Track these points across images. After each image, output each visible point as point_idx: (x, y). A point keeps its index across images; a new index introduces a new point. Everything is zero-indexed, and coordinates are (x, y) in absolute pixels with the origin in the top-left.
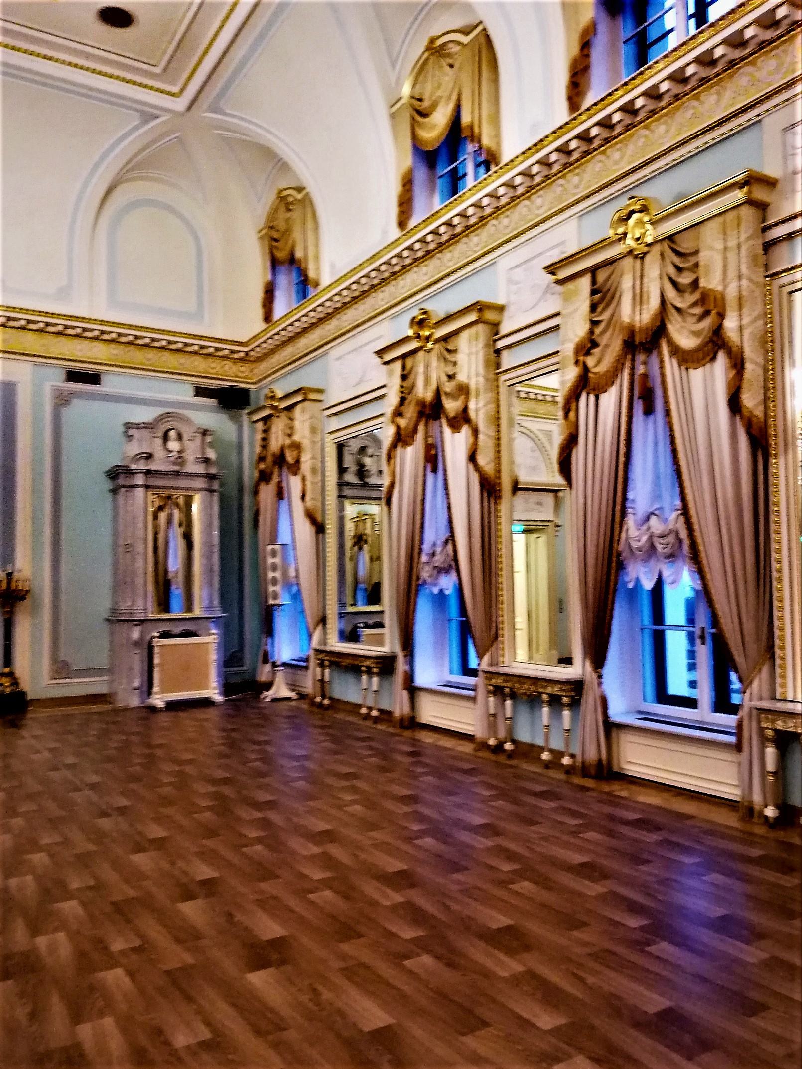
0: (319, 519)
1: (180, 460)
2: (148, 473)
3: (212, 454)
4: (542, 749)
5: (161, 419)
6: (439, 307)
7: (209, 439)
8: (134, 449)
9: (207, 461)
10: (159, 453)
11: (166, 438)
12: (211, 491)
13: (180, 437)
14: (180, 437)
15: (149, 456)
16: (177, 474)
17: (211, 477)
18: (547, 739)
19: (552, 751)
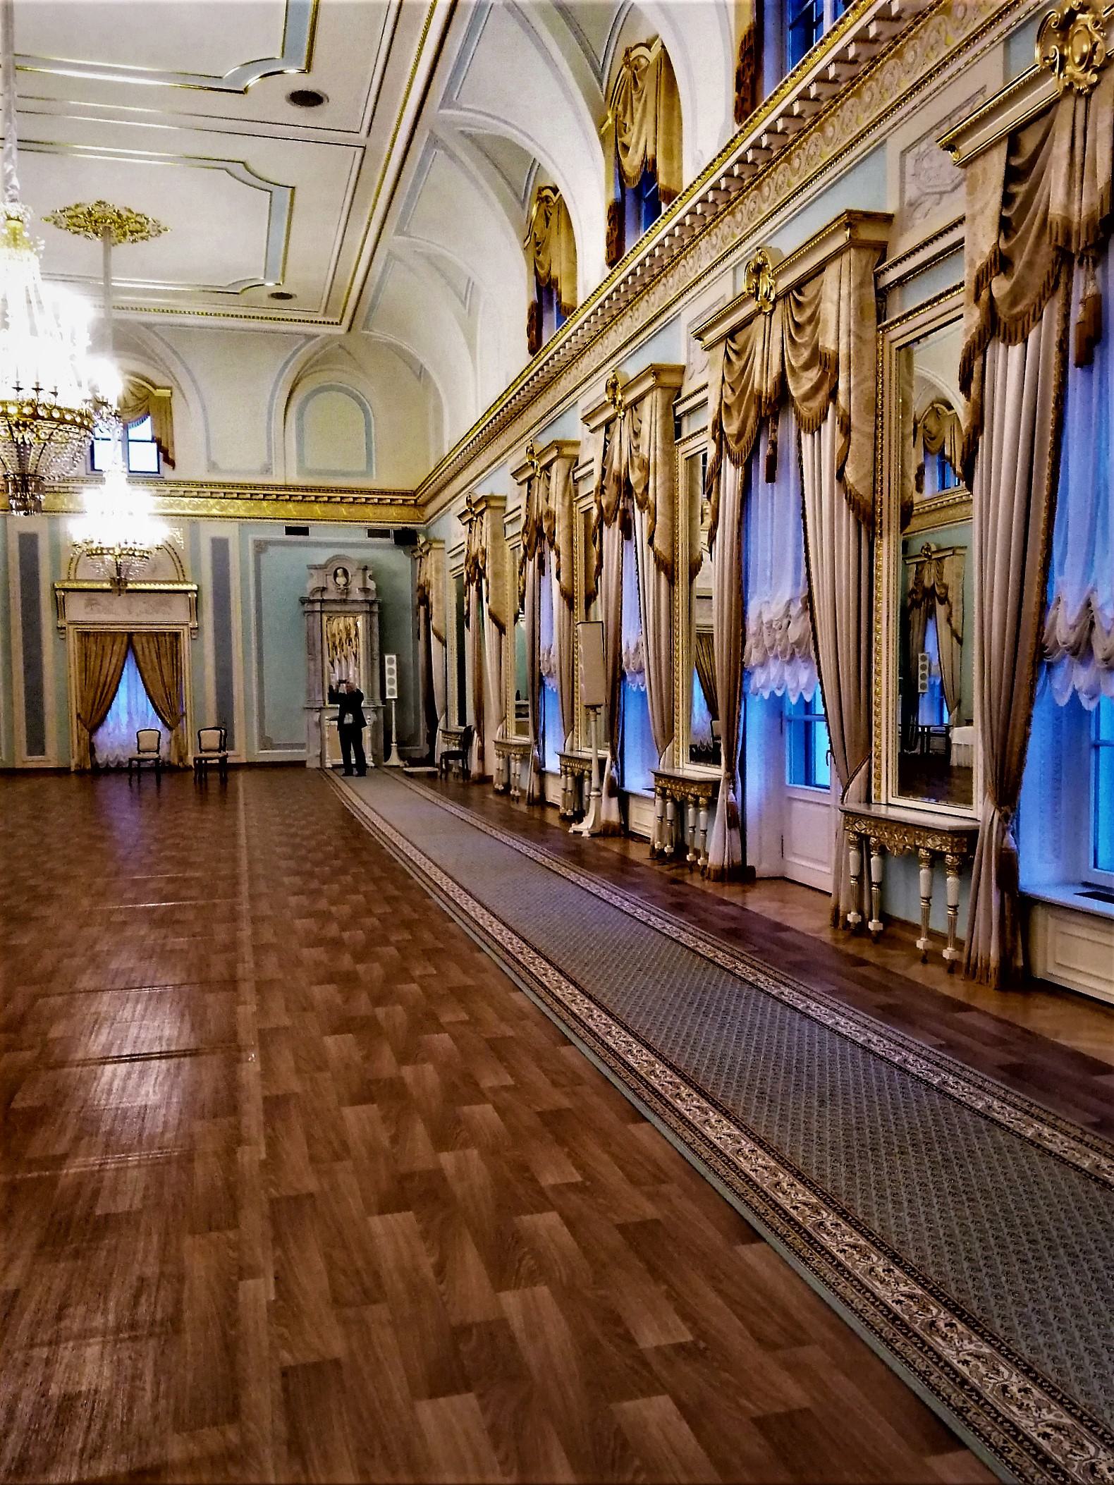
0: (443, 634)
1: (346, 591)
2: (322, 601)
3: (372, 585)
4: (915, 929)
5: (331, 560)
6: (480, 493)
7: (369, 573)
8: (314, 583)
9: (365, 590)
10: (331, 586)
11: (336, 575)
12: (371, 613)
13: (345, 573)
14: (345, 573)
15: (324, 589)
16: (344, 602)
17: (371, 603)
18: (926, 914)
19: (932, 935)
